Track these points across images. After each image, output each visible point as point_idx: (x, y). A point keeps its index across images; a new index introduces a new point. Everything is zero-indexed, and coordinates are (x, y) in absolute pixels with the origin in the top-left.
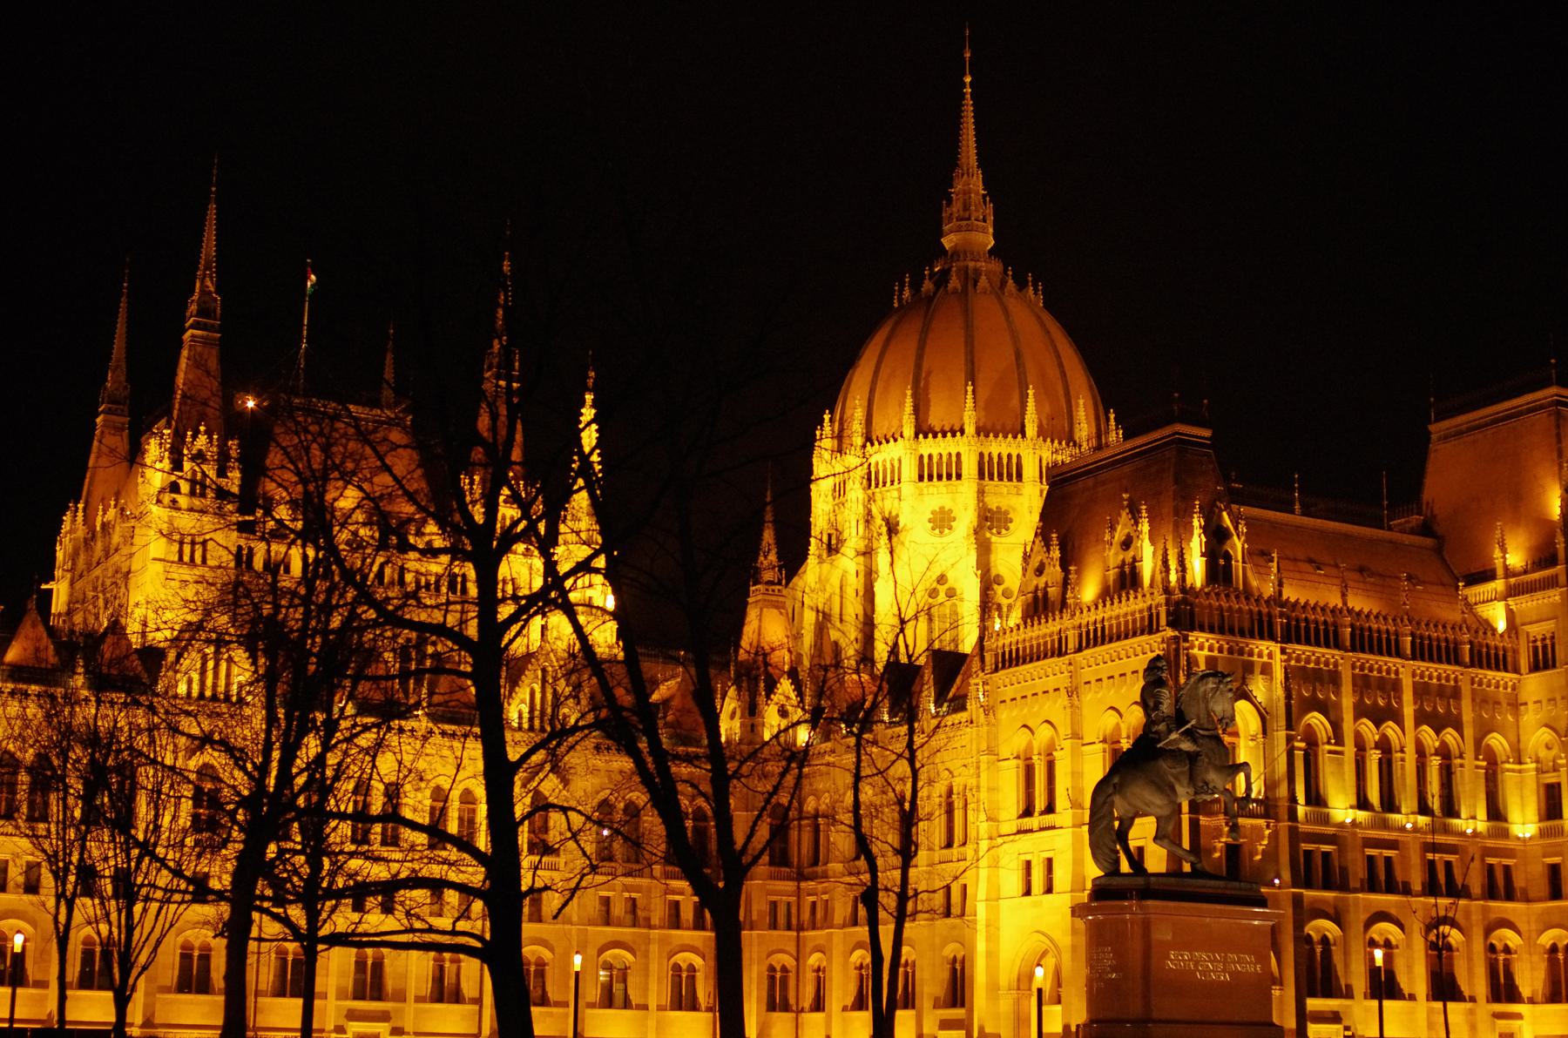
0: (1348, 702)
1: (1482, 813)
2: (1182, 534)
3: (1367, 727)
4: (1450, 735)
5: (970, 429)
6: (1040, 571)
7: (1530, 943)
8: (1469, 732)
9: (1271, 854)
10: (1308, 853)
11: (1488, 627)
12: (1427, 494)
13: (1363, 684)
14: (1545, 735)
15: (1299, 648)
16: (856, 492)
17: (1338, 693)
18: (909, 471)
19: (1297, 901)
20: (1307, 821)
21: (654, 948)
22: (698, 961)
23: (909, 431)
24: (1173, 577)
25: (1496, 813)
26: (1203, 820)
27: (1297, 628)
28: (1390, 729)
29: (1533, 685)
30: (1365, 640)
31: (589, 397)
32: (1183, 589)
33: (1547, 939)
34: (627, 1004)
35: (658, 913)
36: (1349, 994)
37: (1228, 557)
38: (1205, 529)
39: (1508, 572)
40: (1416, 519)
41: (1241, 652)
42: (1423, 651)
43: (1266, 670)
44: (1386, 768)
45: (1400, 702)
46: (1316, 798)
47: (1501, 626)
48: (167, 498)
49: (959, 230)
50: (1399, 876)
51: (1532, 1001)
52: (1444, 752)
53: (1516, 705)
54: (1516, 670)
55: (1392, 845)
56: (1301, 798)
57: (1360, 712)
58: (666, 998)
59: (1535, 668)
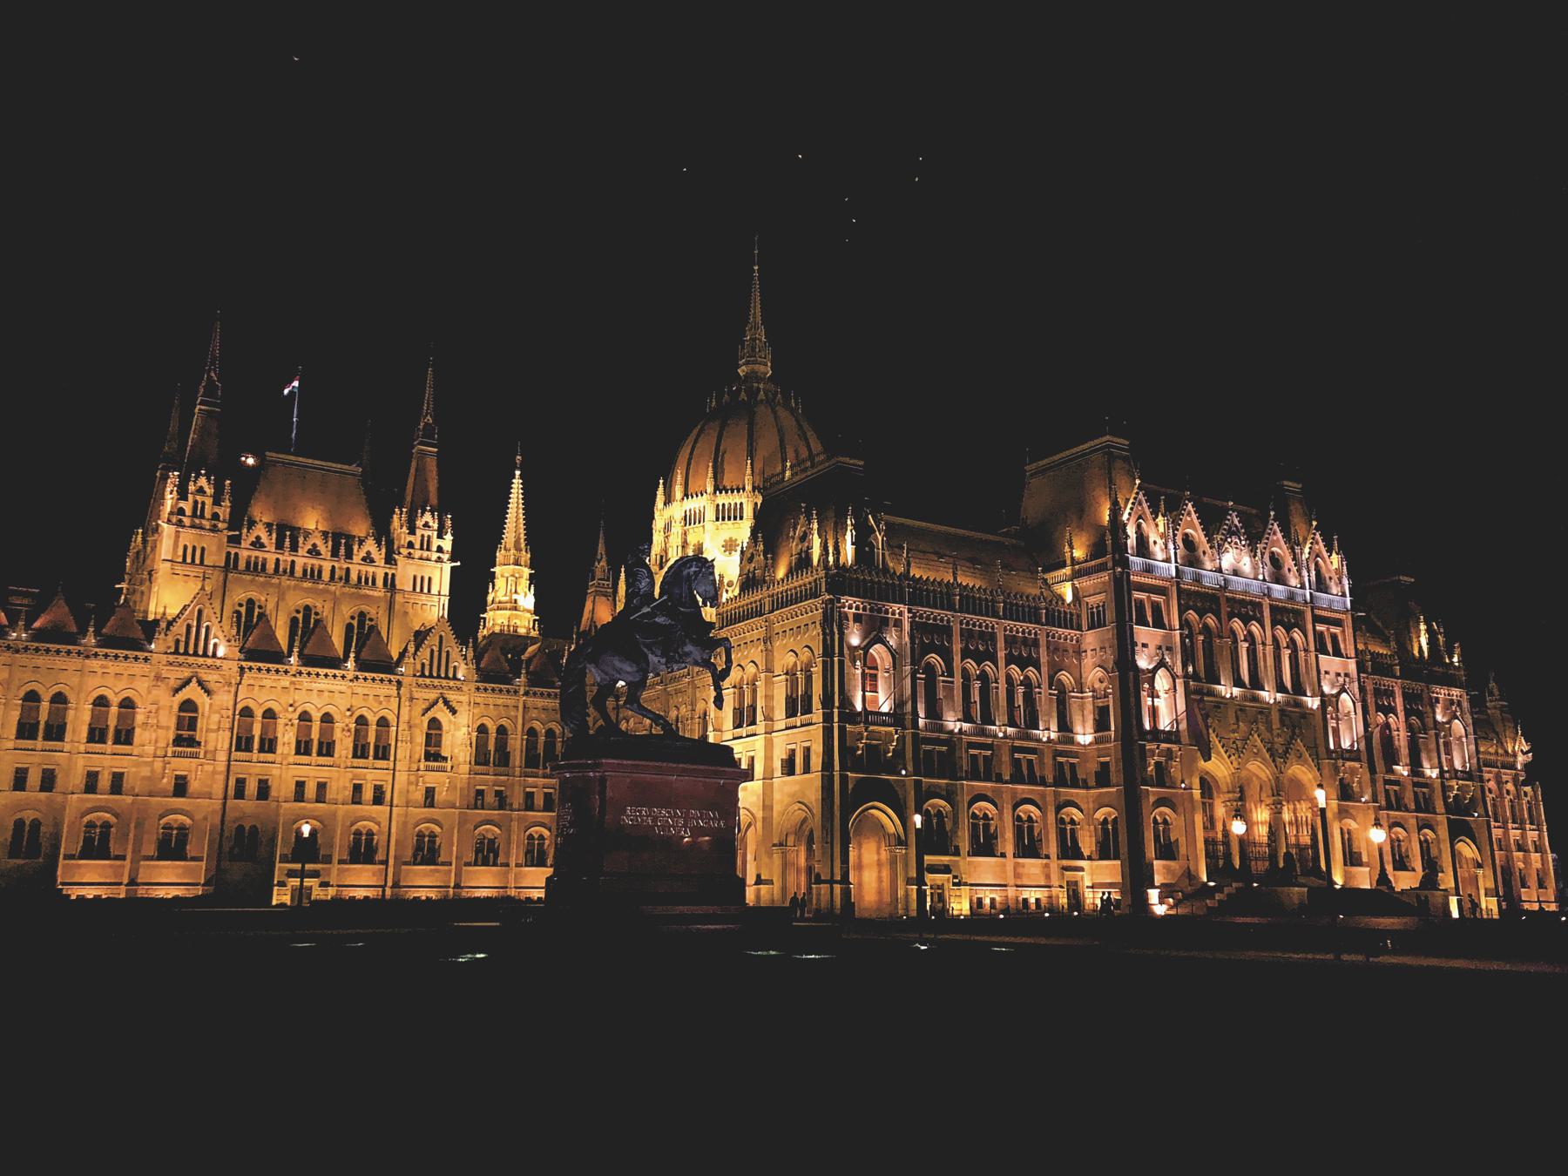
0: (957, 647)
1: (1054, 727)
2: (840, 529)
3: (971, 664)
4: (1031, 672)
5: (748, 488)
6: (750, 560)
7: (1089, 817)
8: (1044, 669)
9: (899, 753)
11: (1061, 598)
13: (967, 635)
14: (1099, 672)
16: (677, 529)
18: (710, 514)
19: (918, 784)
21: (515, 825)
22: (546, 833)
23: (710, 489)
24: (831, 559)
25: (1065, 726)
27: (918, 594)
28: (988, 667)
29: (1091, 639)
30: (970, 602)
31: (518, 473)
33: (1100, 814)
34: (495, 864)
35: (517, 800)
36: (957, 853)
37: (872, 546)
38: (855, 527)
39: (1074, 561)
41: (879, 610)
42: (1013, 613)
43: (898, 624)
44: (985, 692)
46: (934, 713)
47: (1069, 598)
48: (174, 520)
49: (747, 363)
51: (1090, 858)
52: (1027, 683)
53: (1079, 652)
54: (1079, 628)
56: (922, 714)
57: (966, 654)
58: (521, 860)
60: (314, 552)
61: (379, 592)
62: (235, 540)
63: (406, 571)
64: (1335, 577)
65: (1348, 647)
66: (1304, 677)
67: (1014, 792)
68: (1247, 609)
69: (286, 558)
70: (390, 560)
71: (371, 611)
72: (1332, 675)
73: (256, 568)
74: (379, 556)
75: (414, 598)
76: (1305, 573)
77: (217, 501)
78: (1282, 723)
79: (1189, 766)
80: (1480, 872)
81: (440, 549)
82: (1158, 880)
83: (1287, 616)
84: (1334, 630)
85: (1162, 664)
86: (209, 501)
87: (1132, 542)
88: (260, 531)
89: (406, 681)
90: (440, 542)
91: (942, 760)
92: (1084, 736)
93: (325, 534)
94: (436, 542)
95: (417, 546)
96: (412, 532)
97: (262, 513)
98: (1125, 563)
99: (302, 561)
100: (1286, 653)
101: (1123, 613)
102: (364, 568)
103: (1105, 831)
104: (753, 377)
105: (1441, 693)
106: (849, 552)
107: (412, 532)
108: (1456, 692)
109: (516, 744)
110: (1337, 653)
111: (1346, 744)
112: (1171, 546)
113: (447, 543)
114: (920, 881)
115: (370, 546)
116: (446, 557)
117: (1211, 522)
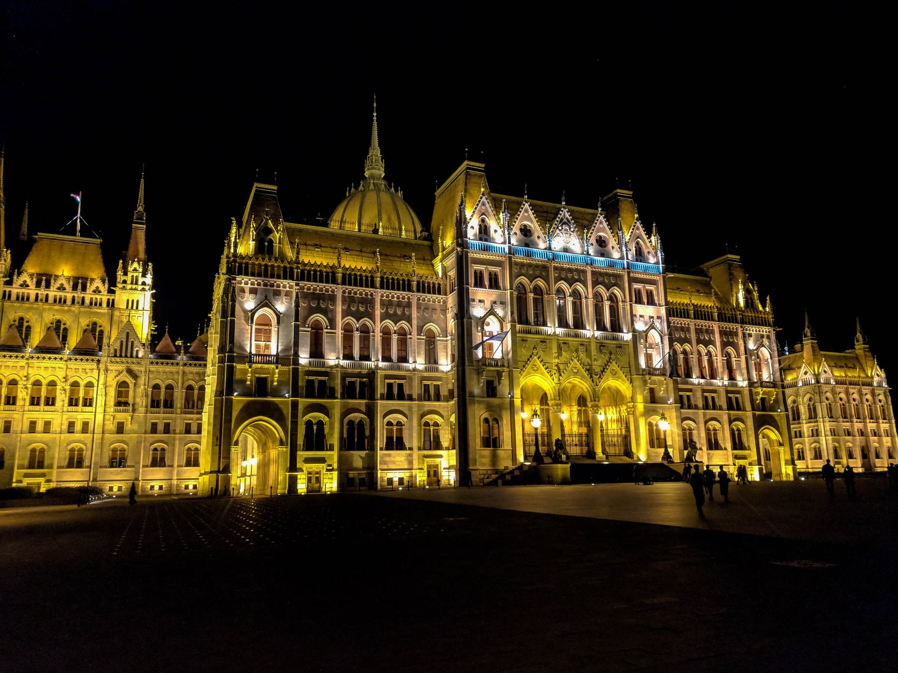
0: (339, 308)
4: (404, 324)
13: (349, 300)
15: (308, 284)
19: (295, 405)
41: (272, 285)
45: (373, 308)
49: (369, 169)
57: (345, 314)
61: (104, 310)
63: (122, 297)
65: (659, 297)
68: (573, 275)
70: (111, 292)
71: (100, 321)
72: (647, 318)
74: (104, 289)
80: (781, 449)
81: (144, 284)
84: (649, 287)
89: (103, 359)
100: (607, 305)
102: (94, 297)
104: (372, 177)
105: (753, 330)
107: (125, 274)
108: (765, 330)
110: (651, 302)
113: (149, 279)
115: (98, 283)
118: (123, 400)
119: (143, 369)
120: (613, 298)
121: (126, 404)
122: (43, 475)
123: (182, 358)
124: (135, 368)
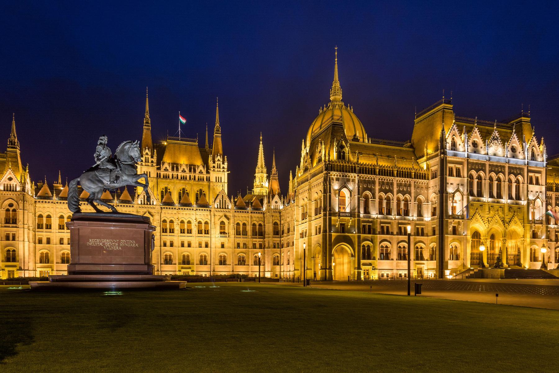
0: (377, 188)
1: (415, 215)
3: (383, 194)
4: (407, 196)
6: (306, 162)
8: (413, 195)
10: (364, 226)
11: (422, 168)
12: (412, 139)
13: (382, 184)
15: (363, 175)
17: (374, 186)
20: (364, 217)
24: (327, 158)
25: (420, 214)
26: (333, 218)
32: (329, 161)
36: (374, 259)
37: (344, 153)
40: (409, 144)
41: (346, 176)
43: (353, 181)
45: (393, 187)
46: (367, 211)
47: (425, 168)
49: (333, 95)
50: (390, 231)
53: (427, 188)
54: (428, 179)
55: (389, 223)
57: (380, 190)
59: (433, 178)
60: (184, 171)
61: (205, 183)
62: (159, 169)
63: (213, 176)
64: (540, 154)
65: (542, 181)
66: (521, 194)
67: (398, 238)
68: (497, 169)
69: (175, 173)
70: (208, 172)
71: (204, 189)
72: (534, 192)
73: (166, 177)
74: (204, 171)
75: (216, 184)
76: (526, 153)
77: (152, 157)
78: (509, 211)
79: (466, 227)
81: (223, 168)
82: (450, 267)
83: (516, 171)
84: (537, 175)
85: (458, 190)
86: (150, 157)
87: (449, 146)
88: (166, 165)
89: (212, 210)
90: (223, 165)
91: (368, 228)
92: (427, 217)
93: (187, 165)
94: (222, 166)
95: (216, 167)
96: (214, 162)
97: (167, 159)
98: (444, 153)
99: (180, 174)
100: (514, 185)
101: (443, 173)
102: (200, 175)
103: (433, 250)
104: (335, 100)
106: (334, 156)
107: (214, 162)
109: (249, 228)
110: (537, 183)
111: (537, 217)
112: (466, 145)
113: (226, 165)
114: (359, 268)
115: (201, 168)
116: (226, 170)
117: (485, 136)
118: (223, 231)
119: (232, 215)
120: (518, 182)
121: (224, 233)
122: (190, 268)
123: (249, 209)
124: (228, 214)
